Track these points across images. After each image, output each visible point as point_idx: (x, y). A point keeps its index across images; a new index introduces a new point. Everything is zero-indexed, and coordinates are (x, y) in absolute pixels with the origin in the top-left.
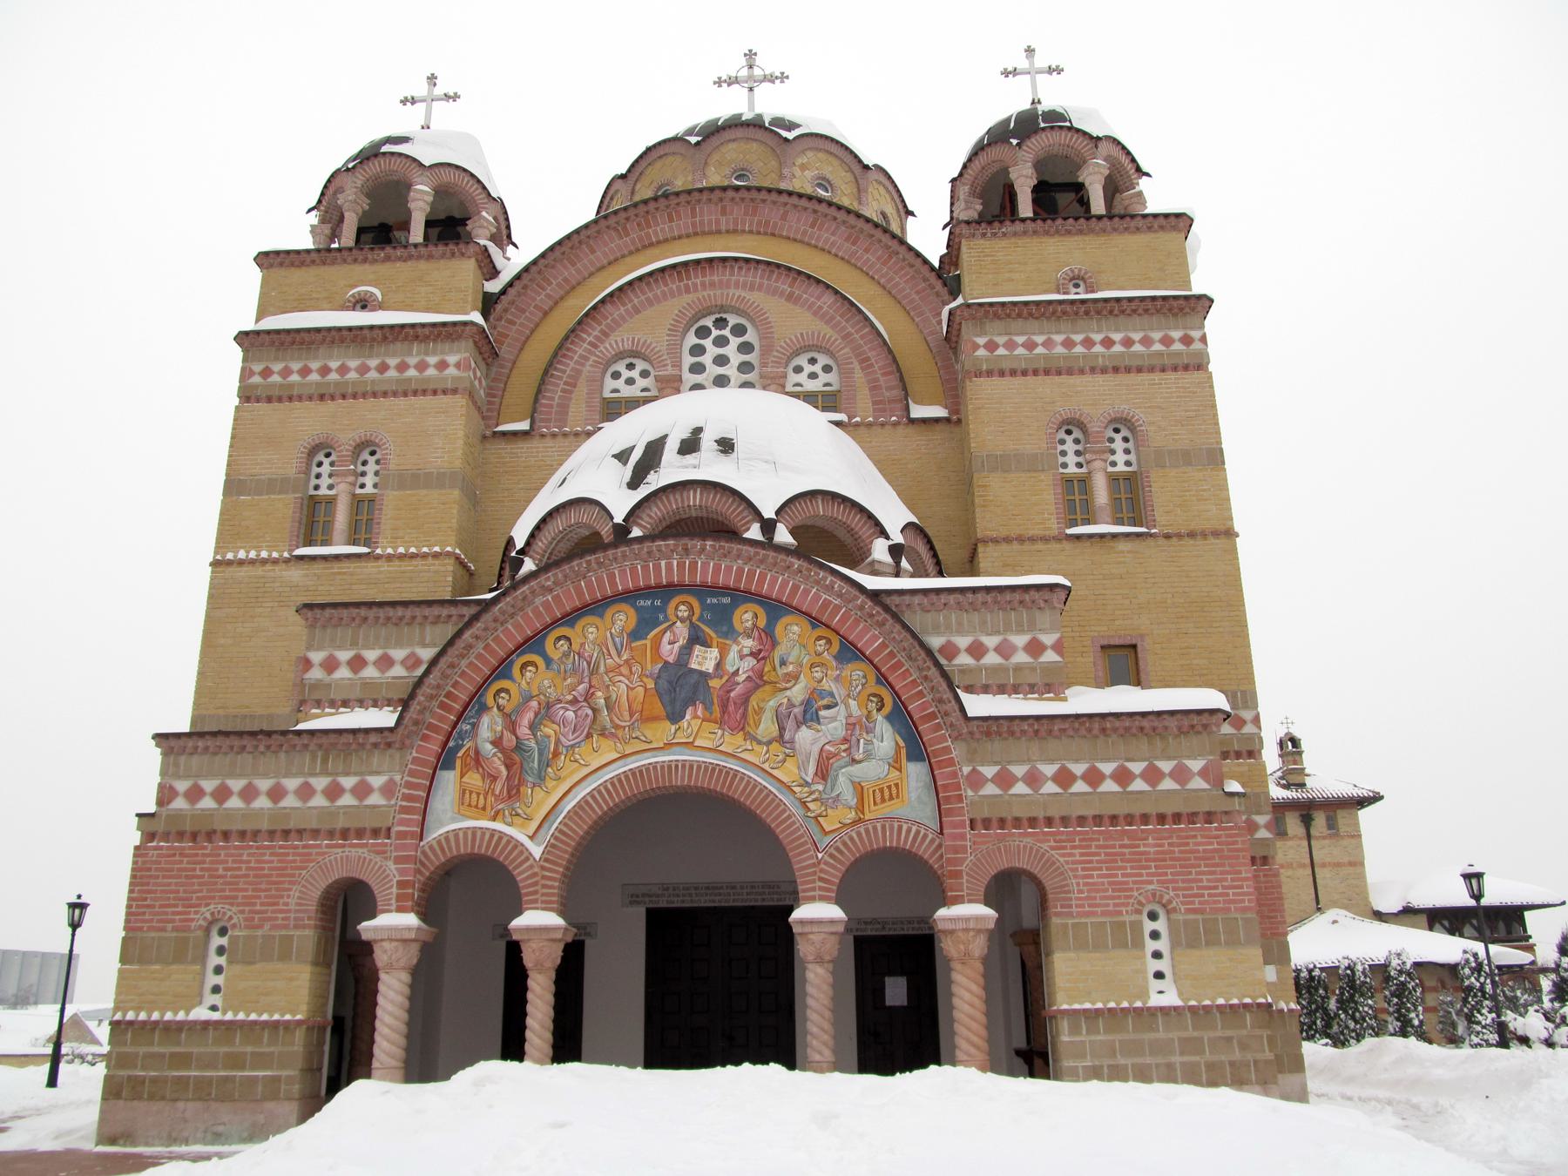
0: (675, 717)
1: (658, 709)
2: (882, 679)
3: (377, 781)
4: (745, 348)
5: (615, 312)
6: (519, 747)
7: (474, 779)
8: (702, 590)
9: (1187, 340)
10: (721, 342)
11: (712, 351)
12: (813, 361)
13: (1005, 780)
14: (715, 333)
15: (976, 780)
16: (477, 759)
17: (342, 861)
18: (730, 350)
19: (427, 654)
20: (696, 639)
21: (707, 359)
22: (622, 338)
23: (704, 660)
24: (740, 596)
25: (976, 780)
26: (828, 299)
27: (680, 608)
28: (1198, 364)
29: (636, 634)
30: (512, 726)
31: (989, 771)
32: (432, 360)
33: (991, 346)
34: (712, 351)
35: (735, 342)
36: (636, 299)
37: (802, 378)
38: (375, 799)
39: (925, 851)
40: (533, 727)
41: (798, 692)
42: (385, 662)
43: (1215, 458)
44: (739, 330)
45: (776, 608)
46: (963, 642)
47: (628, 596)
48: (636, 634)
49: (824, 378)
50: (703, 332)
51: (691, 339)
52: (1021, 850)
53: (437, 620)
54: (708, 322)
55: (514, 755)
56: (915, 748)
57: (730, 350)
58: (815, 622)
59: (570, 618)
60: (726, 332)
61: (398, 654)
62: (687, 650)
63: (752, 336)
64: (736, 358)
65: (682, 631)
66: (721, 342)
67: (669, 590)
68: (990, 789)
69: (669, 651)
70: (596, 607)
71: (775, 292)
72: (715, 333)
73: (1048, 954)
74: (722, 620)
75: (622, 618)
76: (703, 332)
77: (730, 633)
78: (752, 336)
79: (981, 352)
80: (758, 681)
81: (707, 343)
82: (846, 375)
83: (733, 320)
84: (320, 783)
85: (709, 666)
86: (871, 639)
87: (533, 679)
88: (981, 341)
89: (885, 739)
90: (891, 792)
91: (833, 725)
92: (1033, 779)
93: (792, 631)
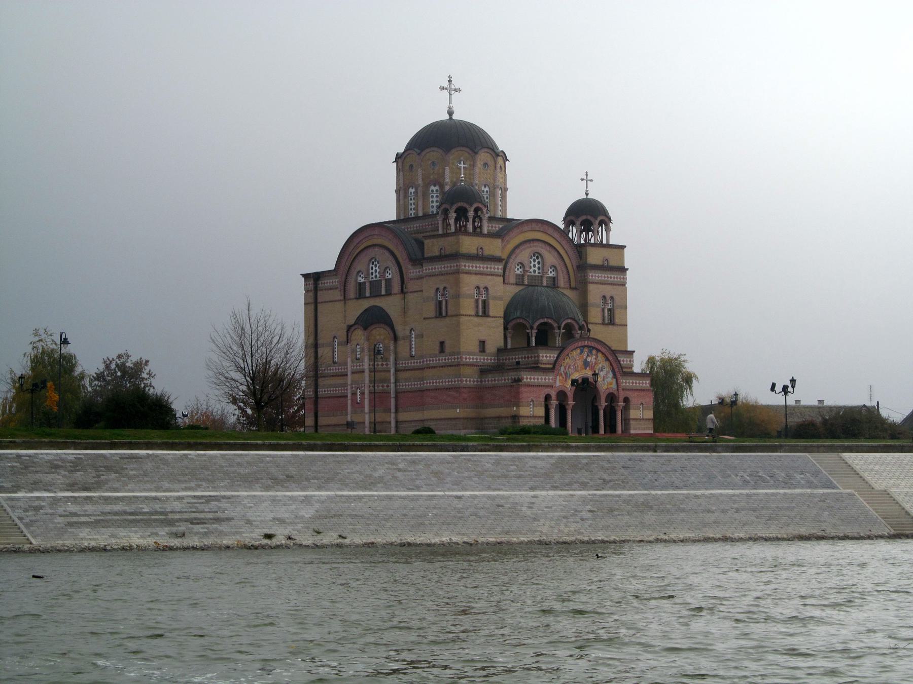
0: (586, 369)
1: (583, 367)
2: (611, 364)
3: (551, 378)
4: (539, 263)
5: (517, 251)
6: (566, 373)
7: (561, 378)
8: (588, 347)
9: (623, 278)
10: (534, 261)
11: (533, 263)
13: (626, 383)
15: (623, 383)
16: (561, 374)
17: (547, 391)
19: (556, 356)
20: (588, 355)
22: (519, 259)
23: (589, 359)
24: (594, 348)
25: (623, 383)
26: (556, 253)
27: (586, 350)
28: (623, 284)
29: (581, 354)
30: (565, 369)
31: (624, 381)
32: (496, 267)
33: (592, 276)
34: (533, 263)
35: (537, 261)
36: (521, 248)
38: (551, 381)
39: (615, 392)
40: (568, 369)
41: (600, 366)
42: (550, 357)
43: (626, 308)
45: (598, 350)
46: (622, 359)
47: (579, 347)
48: (581, 354)
52: (629, 394)
53: (557, 350)
55: (566, 374)
56: (615, 376)
57: (536, 263)
58: (603, 354)
59: (572, 351)
61: (552, 355)
62: (587, 357)
65: (586, 354)
66: (534, 261)
67: (584, 346)
68: (624, 384)
69: (585, 357)
70: (575, 349)
71: (546, 250)
73: (630, 409)
74: (591, 352)
75: (578, 351)
77: (592, 355)
78: (540, 260)
79: (590, 277)
80: (596, 363)
84: (543, 377)
85: (589, 360)
86: (611, 358)
87: (567, 361)
88: (591, 274)
89: (611, 375)
90: (611, 383)
91: (605, 371)
92: (629, 383)
93: (600, 355)
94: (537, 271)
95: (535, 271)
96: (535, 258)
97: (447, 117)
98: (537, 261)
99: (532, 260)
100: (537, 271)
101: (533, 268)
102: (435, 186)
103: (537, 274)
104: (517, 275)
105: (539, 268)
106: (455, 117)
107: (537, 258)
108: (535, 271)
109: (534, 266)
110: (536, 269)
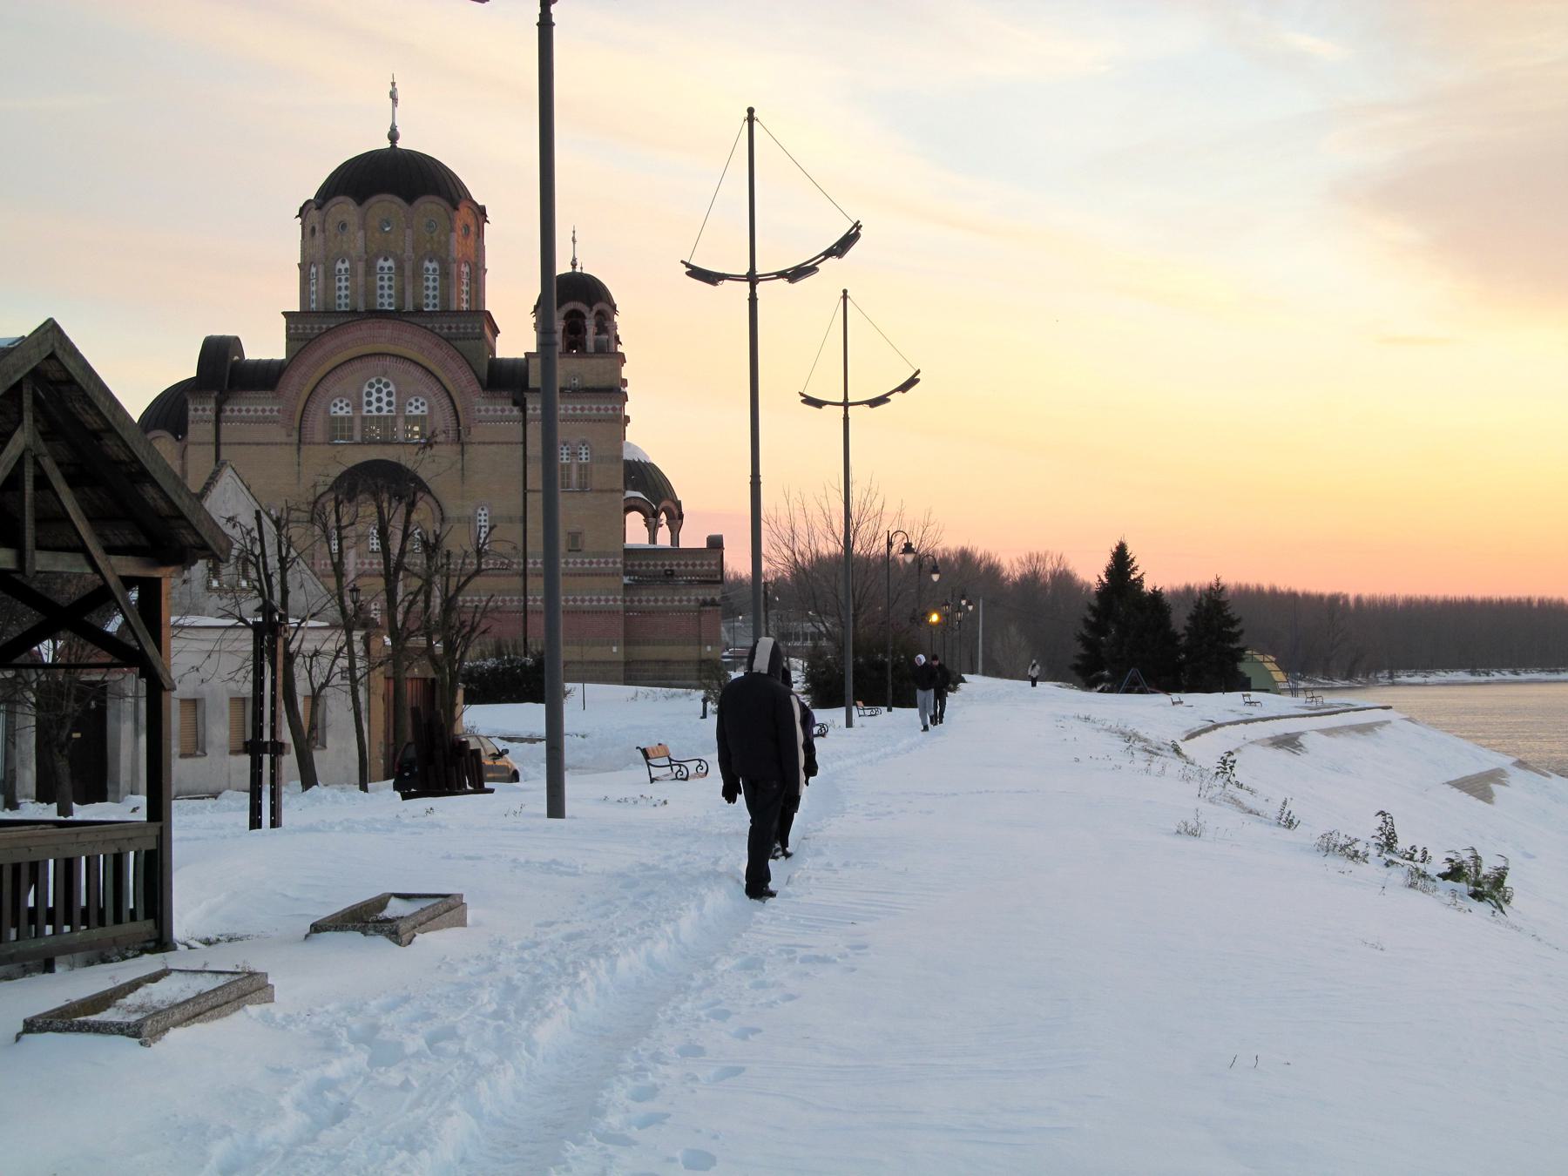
4: (389, 394)
10: (379, 391)
11: (375, 395)
12: (417, 400)
14: (377, 386)
18: (383, 395)
21: (373, 399)
34: (375, 395)
35: (385, 391)
37: (412, 408)
44: (387, 385)
49: (421, 408)
50: (371, 386)
51: (366, 389)
54: (373, 380)
57: (383, 395)
60: (381, 386)
63: (392, 388)
64: (386, 399)
66: (379, 391)
72: (377, 386)
76: (371, 386)
78: (392, 388)
81: (373, 391)
82: (431, 408)
83: (384, 380)
94: (386, 408)
95: (379, 409)
96: (381, 386)
97: (387, 144)
98: (385, 391)
99: (373, 391)
100: (386, 408)
101: (375, 405)
102: (431, 261)
103: (384, 413)
104: (335, 419)
105: (389, 404)
106: (400, 145)
107: (387, 385)
108: (379, 409)
109: (379, 400)
110: (383, 404)
